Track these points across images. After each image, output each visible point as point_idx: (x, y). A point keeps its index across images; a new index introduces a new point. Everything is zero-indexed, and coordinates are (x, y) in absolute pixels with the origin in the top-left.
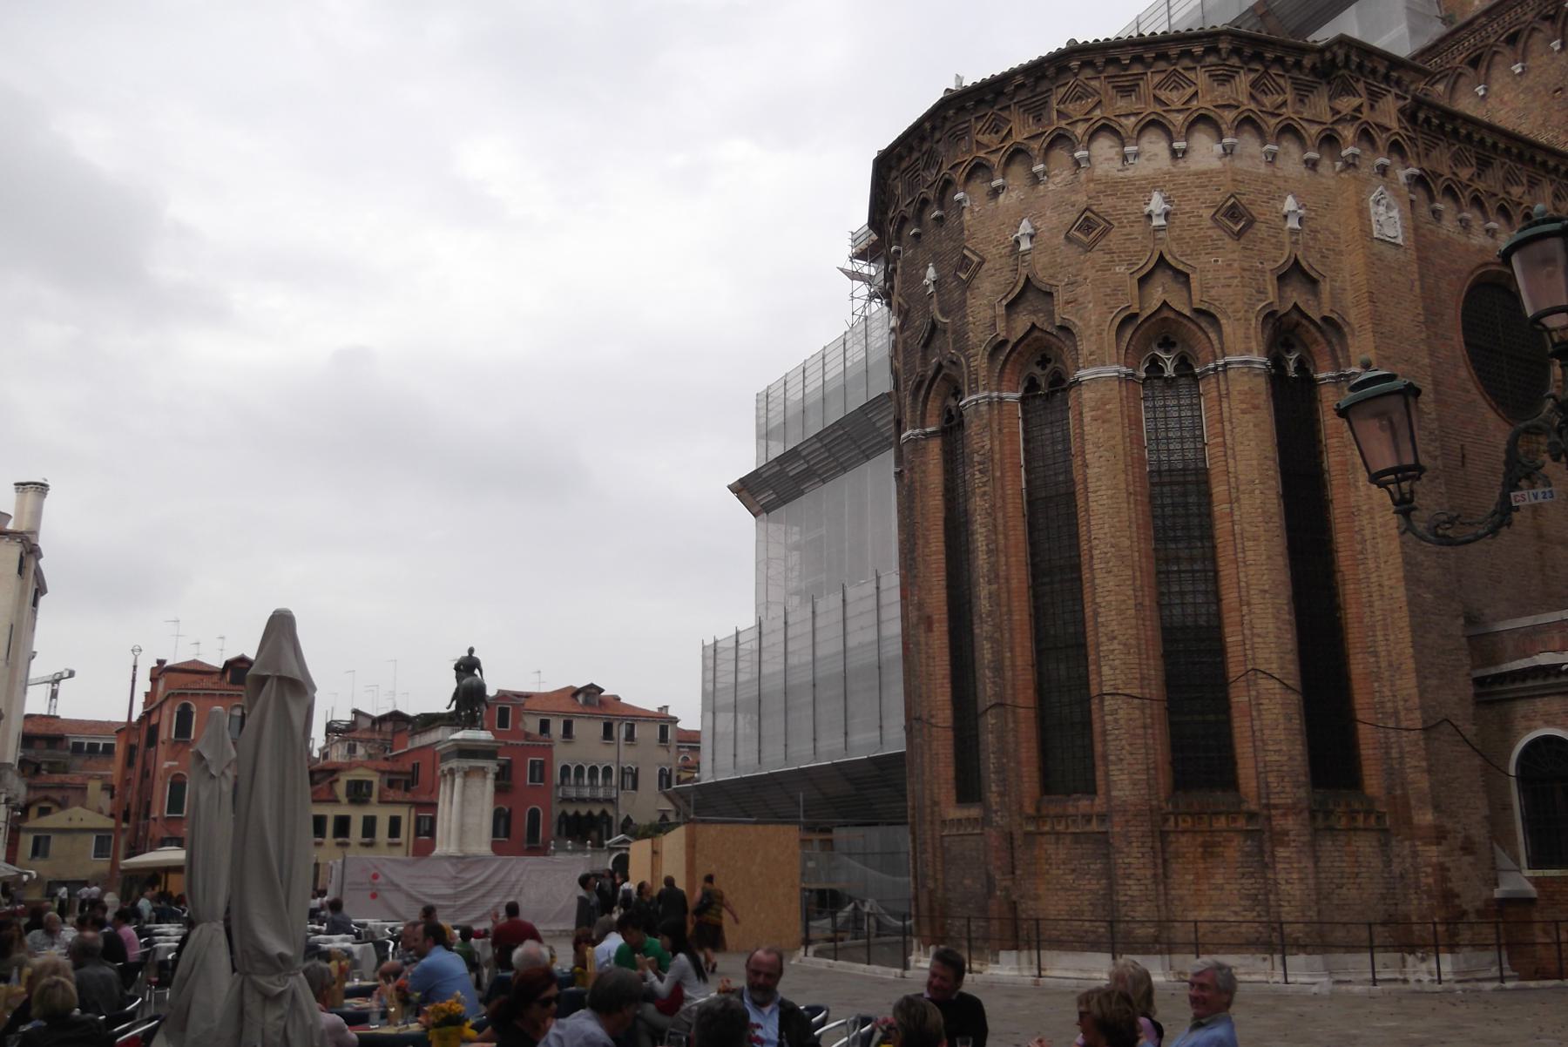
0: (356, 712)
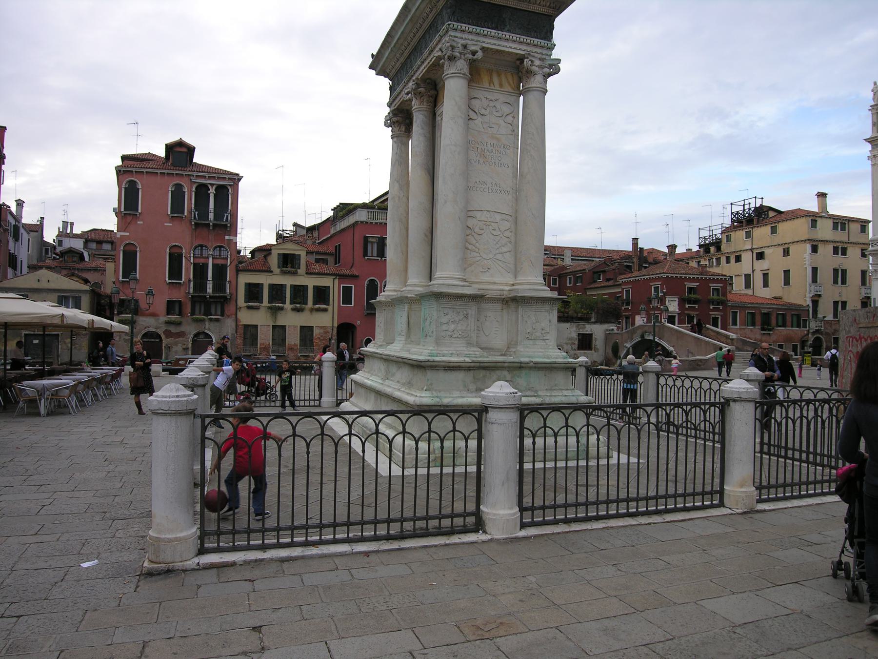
0: (295, 225)
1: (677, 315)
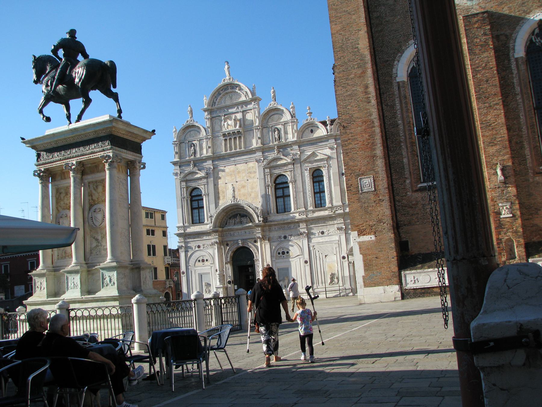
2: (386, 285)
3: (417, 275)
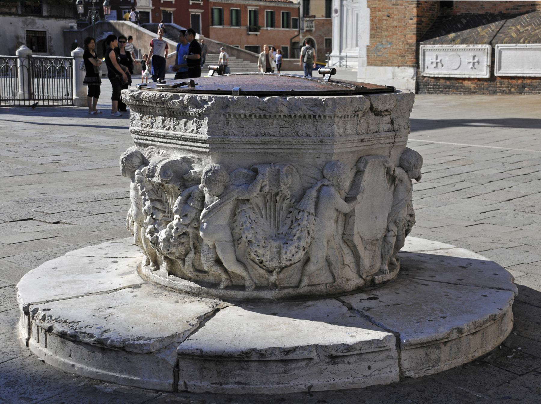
1: (150, 11)
2: (396, 66)
3: (442, 53)
